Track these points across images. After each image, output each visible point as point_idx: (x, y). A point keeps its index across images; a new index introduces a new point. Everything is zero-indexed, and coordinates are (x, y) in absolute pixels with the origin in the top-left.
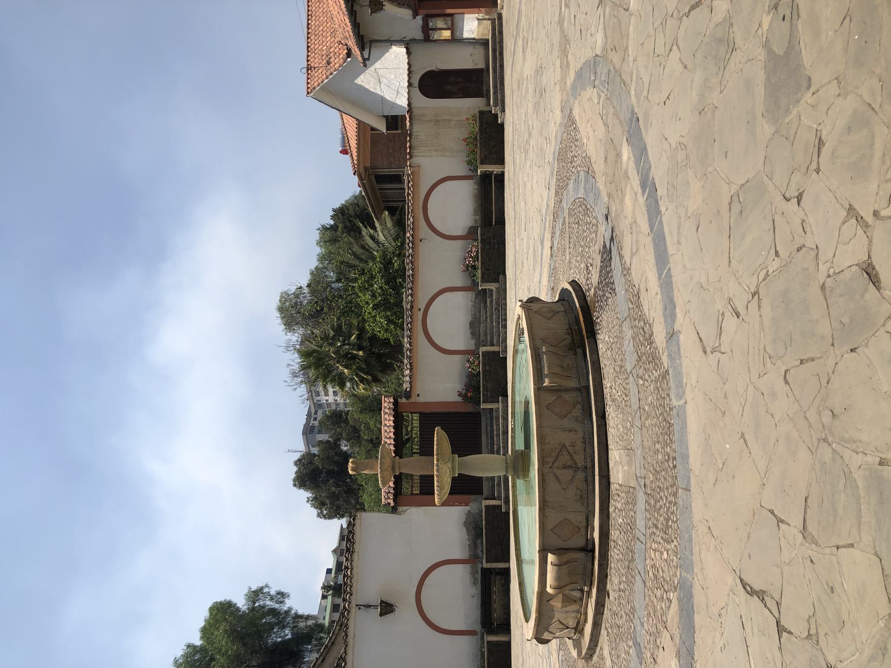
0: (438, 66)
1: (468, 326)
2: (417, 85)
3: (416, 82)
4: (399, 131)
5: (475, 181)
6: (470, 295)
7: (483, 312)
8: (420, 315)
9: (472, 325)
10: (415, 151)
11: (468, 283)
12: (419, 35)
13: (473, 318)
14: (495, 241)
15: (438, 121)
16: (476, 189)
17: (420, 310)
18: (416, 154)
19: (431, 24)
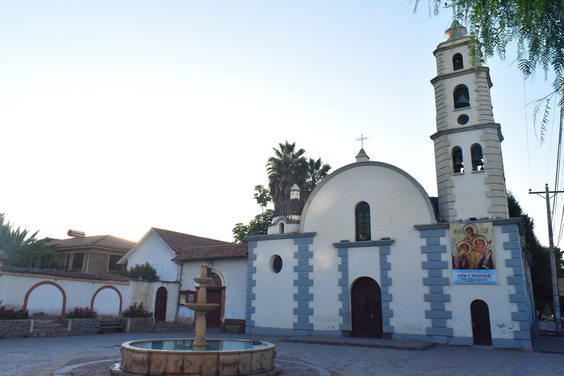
0: (169, 297)
1: (41, 311)
2: (163, 286)
3: (165, 285)
4: (108, 271)
5: (118, 316)
6: (60, 313)
7: (49, 321)
8: (53, 281)
9: (42, 314)
10: (135, 283)
11: (67, 311)
12: (183, 289)
13: (46, 314)
14: (93, 329)
15: (147, 296)
16: (114, 317)
17: (56, 280)
18: (134, 283)
19: (191, 295)
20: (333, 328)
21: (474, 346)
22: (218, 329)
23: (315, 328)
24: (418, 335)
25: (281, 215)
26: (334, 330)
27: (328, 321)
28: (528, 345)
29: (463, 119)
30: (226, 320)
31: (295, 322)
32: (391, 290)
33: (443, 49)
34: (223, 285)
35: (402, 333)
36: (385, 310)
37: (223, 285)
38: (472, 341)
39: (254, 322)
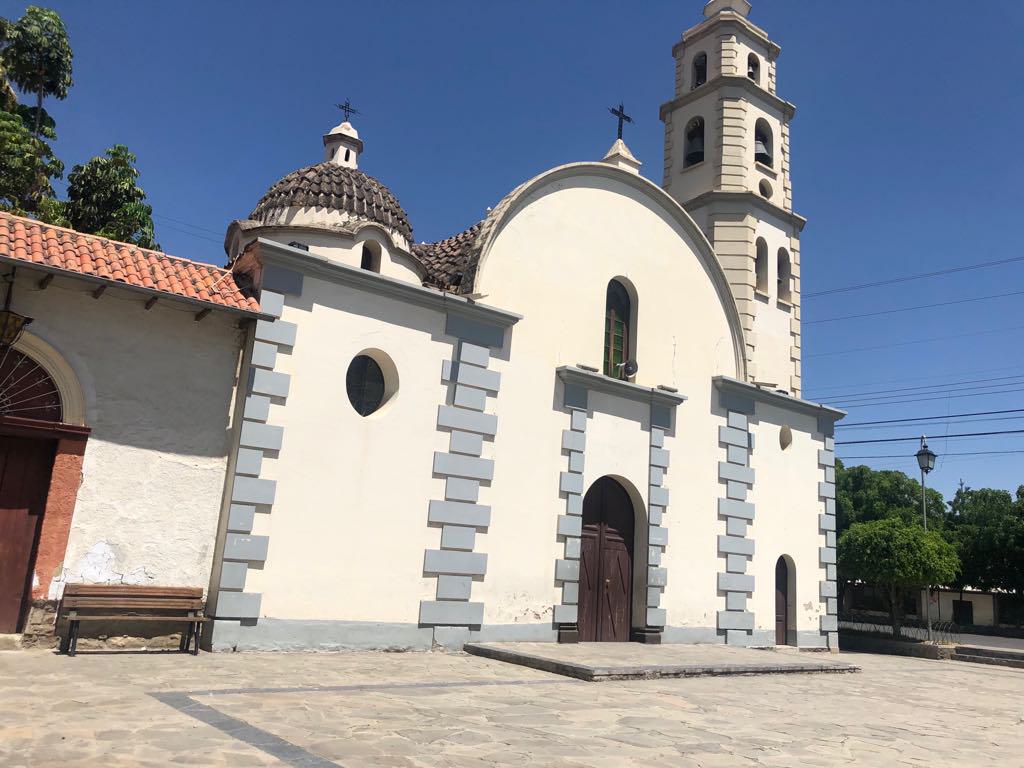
20: (537, 616)
21: (778, 647)
22: (17, 637)
23: (487, 621)
24: (705, 629)
25: (361, 214)
26: (537, 622)
27: (524, 595)
28: (834, 638)
29: (765, 189)
30: (72, 591)
31: (427, 599)
32: (666, 520)
33: (740, 28)
34: (69, 420)
35: (679, 626)
36: (654, 568)
37: (69, 420)
38: (774, 640)
39: (256, 598)
